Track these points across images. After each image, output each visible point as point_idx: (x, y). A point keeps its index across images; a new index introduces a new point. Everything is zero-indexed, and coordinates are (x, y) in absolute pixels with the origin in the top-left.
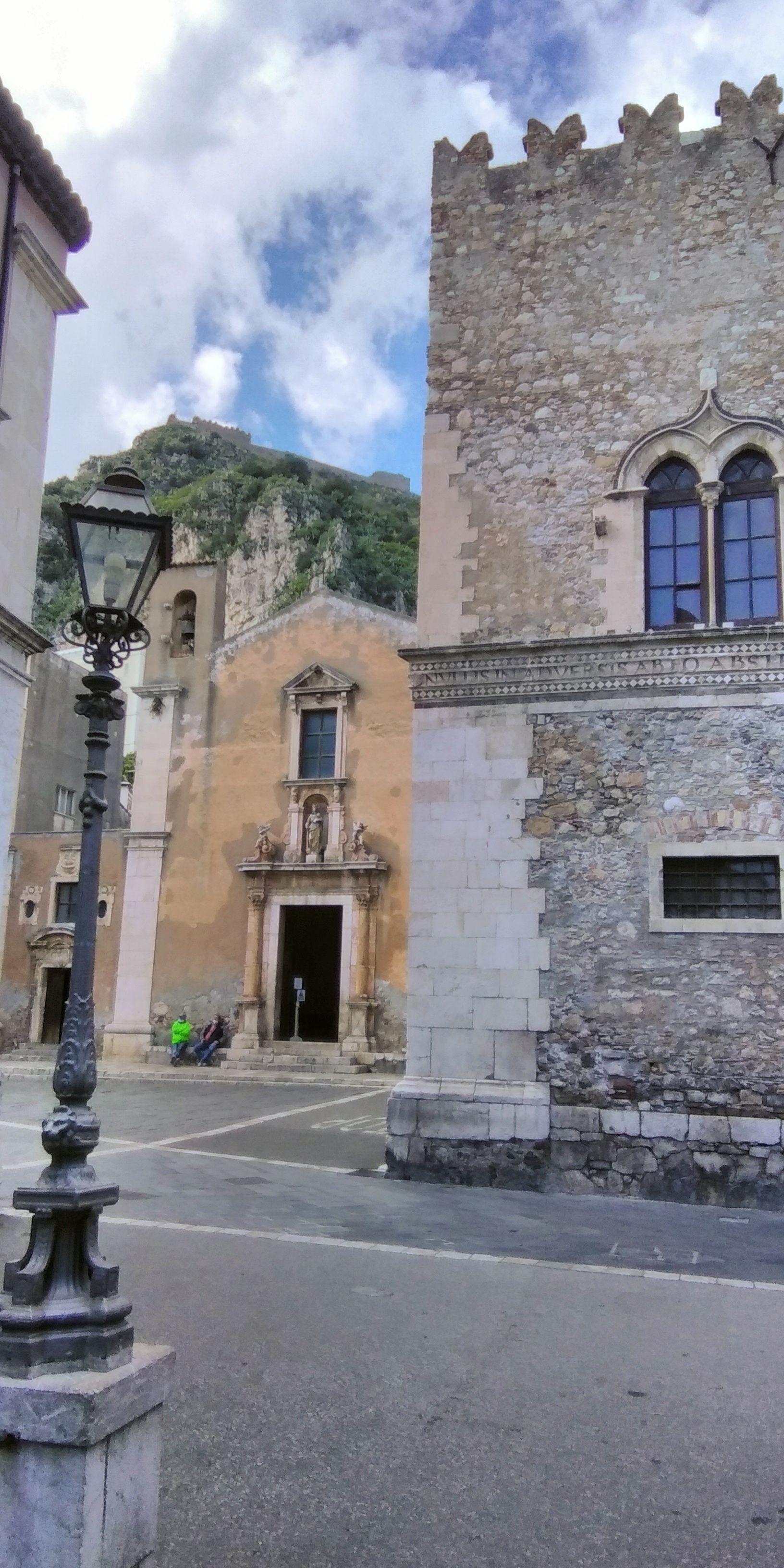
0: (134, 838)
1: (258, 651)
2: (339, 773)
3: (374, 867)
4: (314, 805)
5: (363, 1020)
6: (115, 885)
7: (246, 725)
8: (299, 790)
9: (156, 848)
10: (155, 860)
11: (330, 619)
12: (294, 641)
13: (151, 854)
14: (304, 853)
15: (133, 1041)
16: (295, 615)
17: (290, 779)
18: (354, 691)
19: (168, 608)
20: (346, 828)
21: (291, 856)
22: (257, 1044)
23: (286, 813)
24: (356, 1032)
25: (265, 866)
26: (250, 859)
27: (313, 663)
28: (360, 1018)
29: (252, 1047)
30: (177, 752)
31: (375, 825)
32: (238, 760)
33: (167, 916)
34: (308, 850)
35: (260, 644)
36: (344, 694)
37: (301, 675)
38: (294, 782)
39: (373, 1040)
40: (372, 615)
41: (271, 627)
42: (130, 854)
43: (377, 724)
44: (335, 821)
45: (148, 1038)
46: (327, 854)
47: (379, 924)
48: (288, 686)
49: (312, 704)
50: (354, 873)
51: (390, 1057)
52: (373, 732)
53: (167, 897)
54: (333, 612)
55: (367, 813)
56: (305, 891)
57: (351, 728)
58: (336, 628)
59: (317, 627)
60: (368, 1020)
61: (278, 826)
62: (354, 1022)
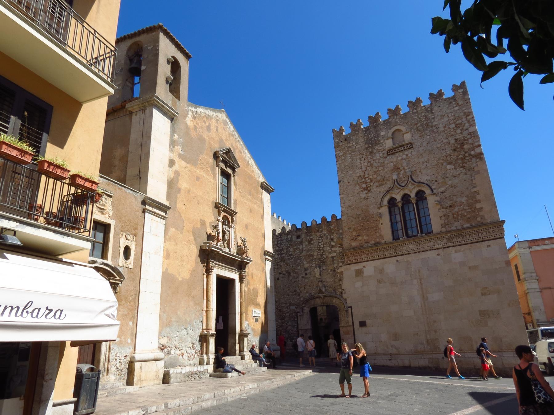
6: (135, 235)
32: (198, 178)
35: (205, 119)
46: (231, 250)
48: (221, 151)
49: (224, 167)
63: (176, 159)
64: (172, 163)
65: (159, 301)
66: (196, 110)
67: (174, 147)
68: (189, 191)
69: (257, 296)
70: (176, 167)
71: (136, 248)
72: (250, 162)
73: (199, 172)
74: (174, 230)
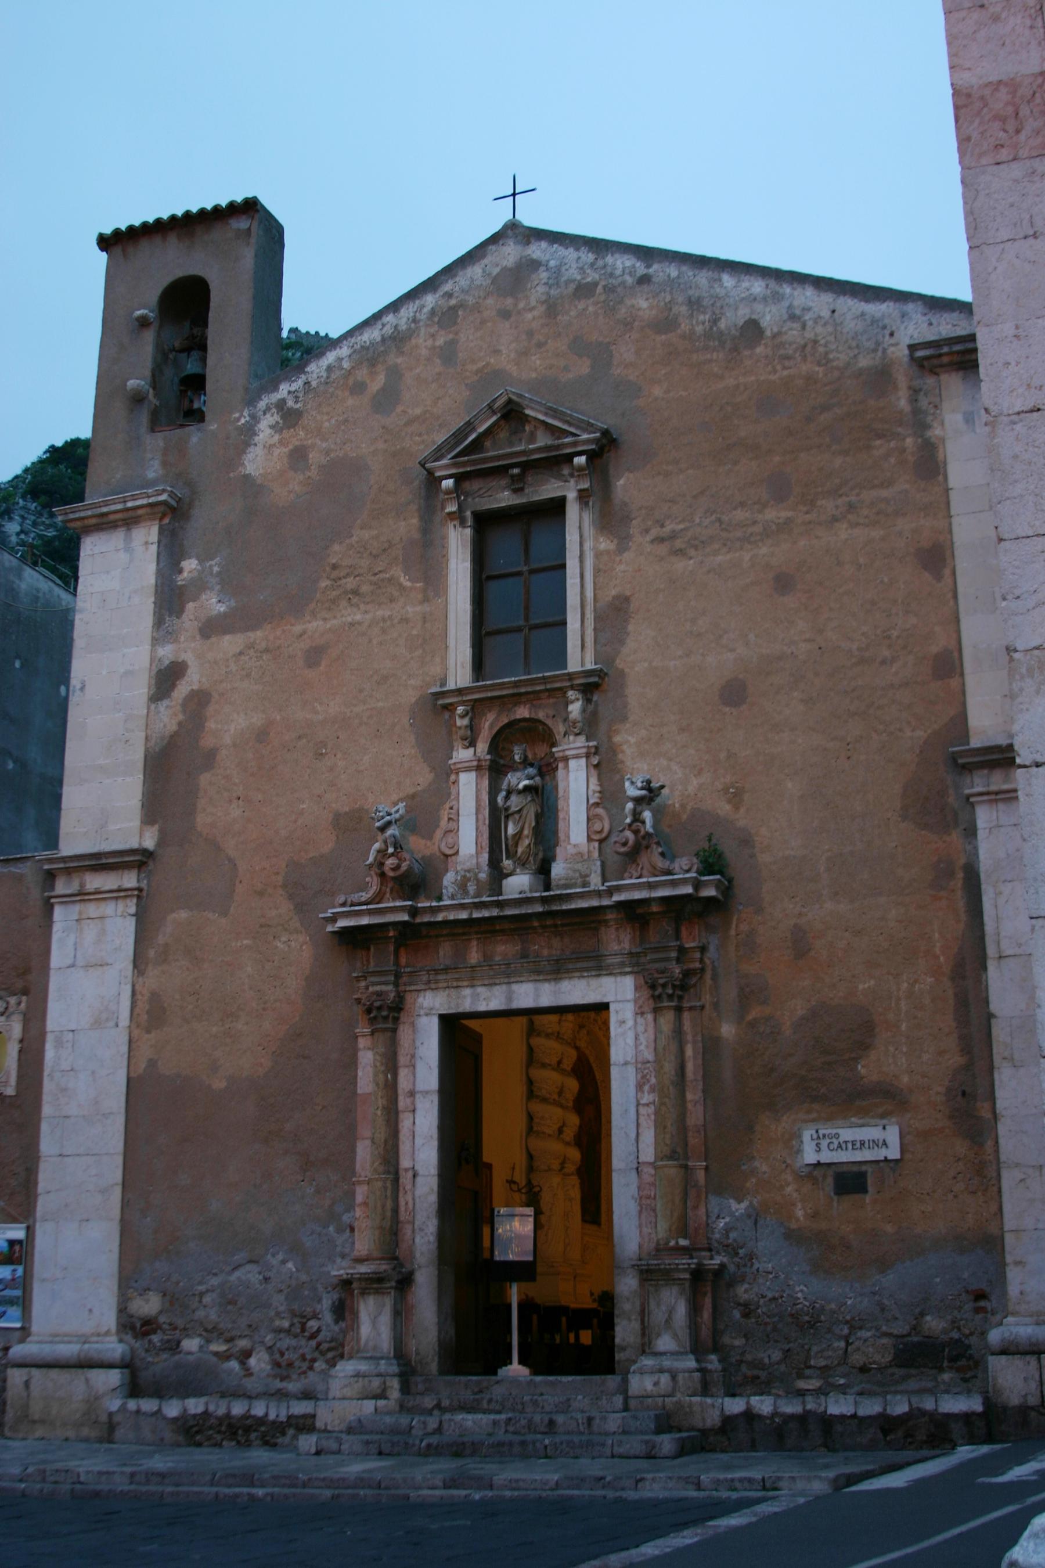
0: (68, 872)
1: (358, 388)
2: (578, 658)
3: (688, 890)
4: (519, 747)
5: (681, 1310)
6: (25, 992)
7: (334, 567)
8: (477, 708)
9: (119, 894)
10: (119, 926)
11: (538, 289)
12: (448, 354)
13: (109, 908)
14: (498, 874)
15: (76, 1387)
16: (449, 295)
17: (451, 685)
18: (605, 449)
19: (143, 323)
20: (608, 796)
21: (462, 886)
22: (395, 1384)
23: (446, 774)
24: (665, 1343)
25: (395, 911)
26: (355, 897)
27: (499, 394)
28: (673, 1304)
29: (382, 1395)
30: (167, 652)
31: (685, 783)
32: (314, 656)
33: (152, 1063)
34: (507, 864)
35: (362, 374)
36: (581, 460)
37: (469, 426)
38: (460, 691)
39: (713, 1362)
40: (641, 268)
41: (388, 330)
42: (58, 912)
43: (670, 527)
44: (576, 784)
45: (114, 1377)
46: (558, 870)
47: (711, 1047)
48: (438, 454)
50: (633, 912)
51: (763, 1405)
52: (663, 549)
53: (150, 1014)
54: (544, 275)
55: (662, 759)
56: (508, 973)
57: (606, 544)
58: (552, 308)
59: (505, 314)
60: (694, 1310)
61: (427, 811)
62: (658, 1315)
63: (184, 648)
64: (166, 678)
65: (117, 1175)
66: (297, 385)
67: (179, 612)
68: (262, 735)
69: (864, 1046)
70: (192, 681)
71: (25, 1029)
72: (769, 317)
73: (315, 626)
74: (183, 915)
